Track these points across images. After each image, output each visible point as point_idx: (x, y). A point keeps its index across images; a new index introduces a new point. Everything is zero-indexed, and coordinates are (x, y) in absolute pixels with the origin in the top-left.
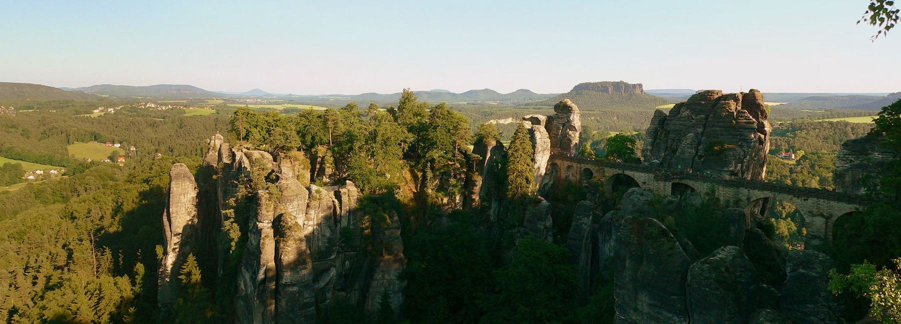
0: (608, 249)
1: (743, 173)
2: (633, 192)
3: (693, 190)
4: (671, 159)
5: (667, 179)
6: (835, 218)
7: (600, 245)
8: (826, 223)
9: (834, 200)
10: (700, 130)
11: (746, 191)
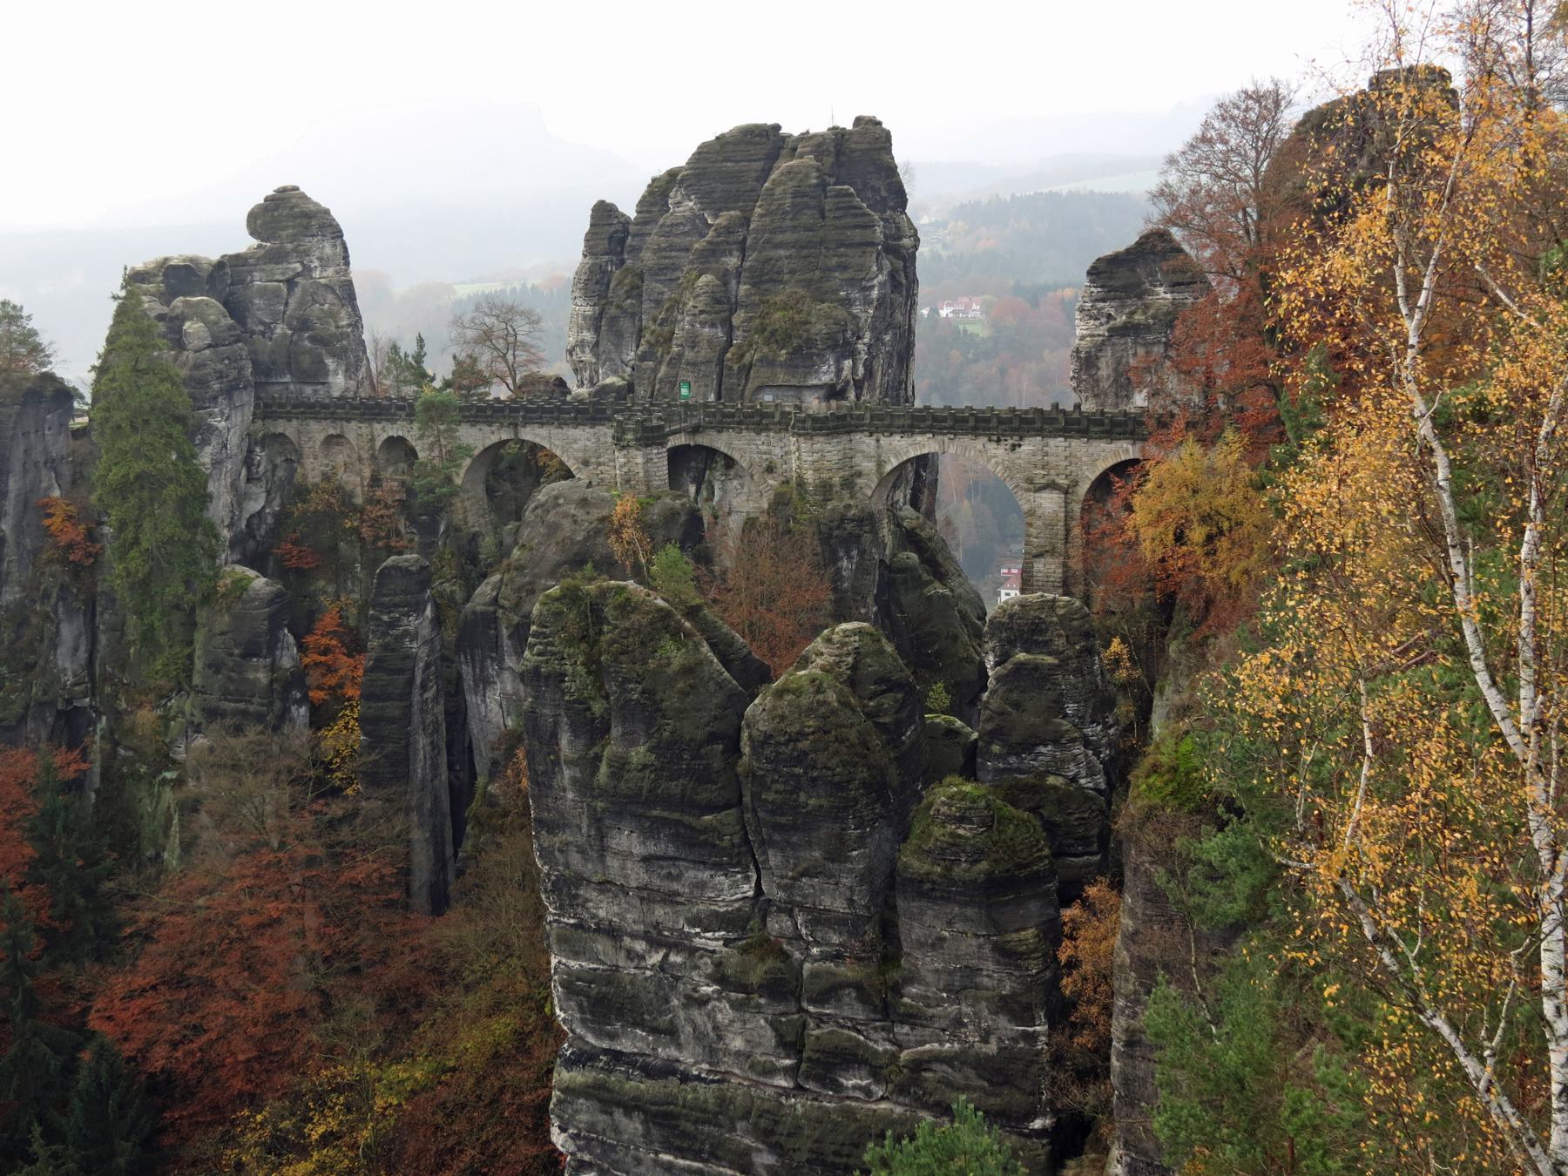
0: (494, 707)
1: (859, 386)
2: (557, 498)
3: (730, 462)
4: (655, 371)
5: (650, 437)
6: (1083, 488)
7: (472, 699)
8: (1066, 503)
9: (1055, 434)
10: (732, 261)
11: (871, 441)
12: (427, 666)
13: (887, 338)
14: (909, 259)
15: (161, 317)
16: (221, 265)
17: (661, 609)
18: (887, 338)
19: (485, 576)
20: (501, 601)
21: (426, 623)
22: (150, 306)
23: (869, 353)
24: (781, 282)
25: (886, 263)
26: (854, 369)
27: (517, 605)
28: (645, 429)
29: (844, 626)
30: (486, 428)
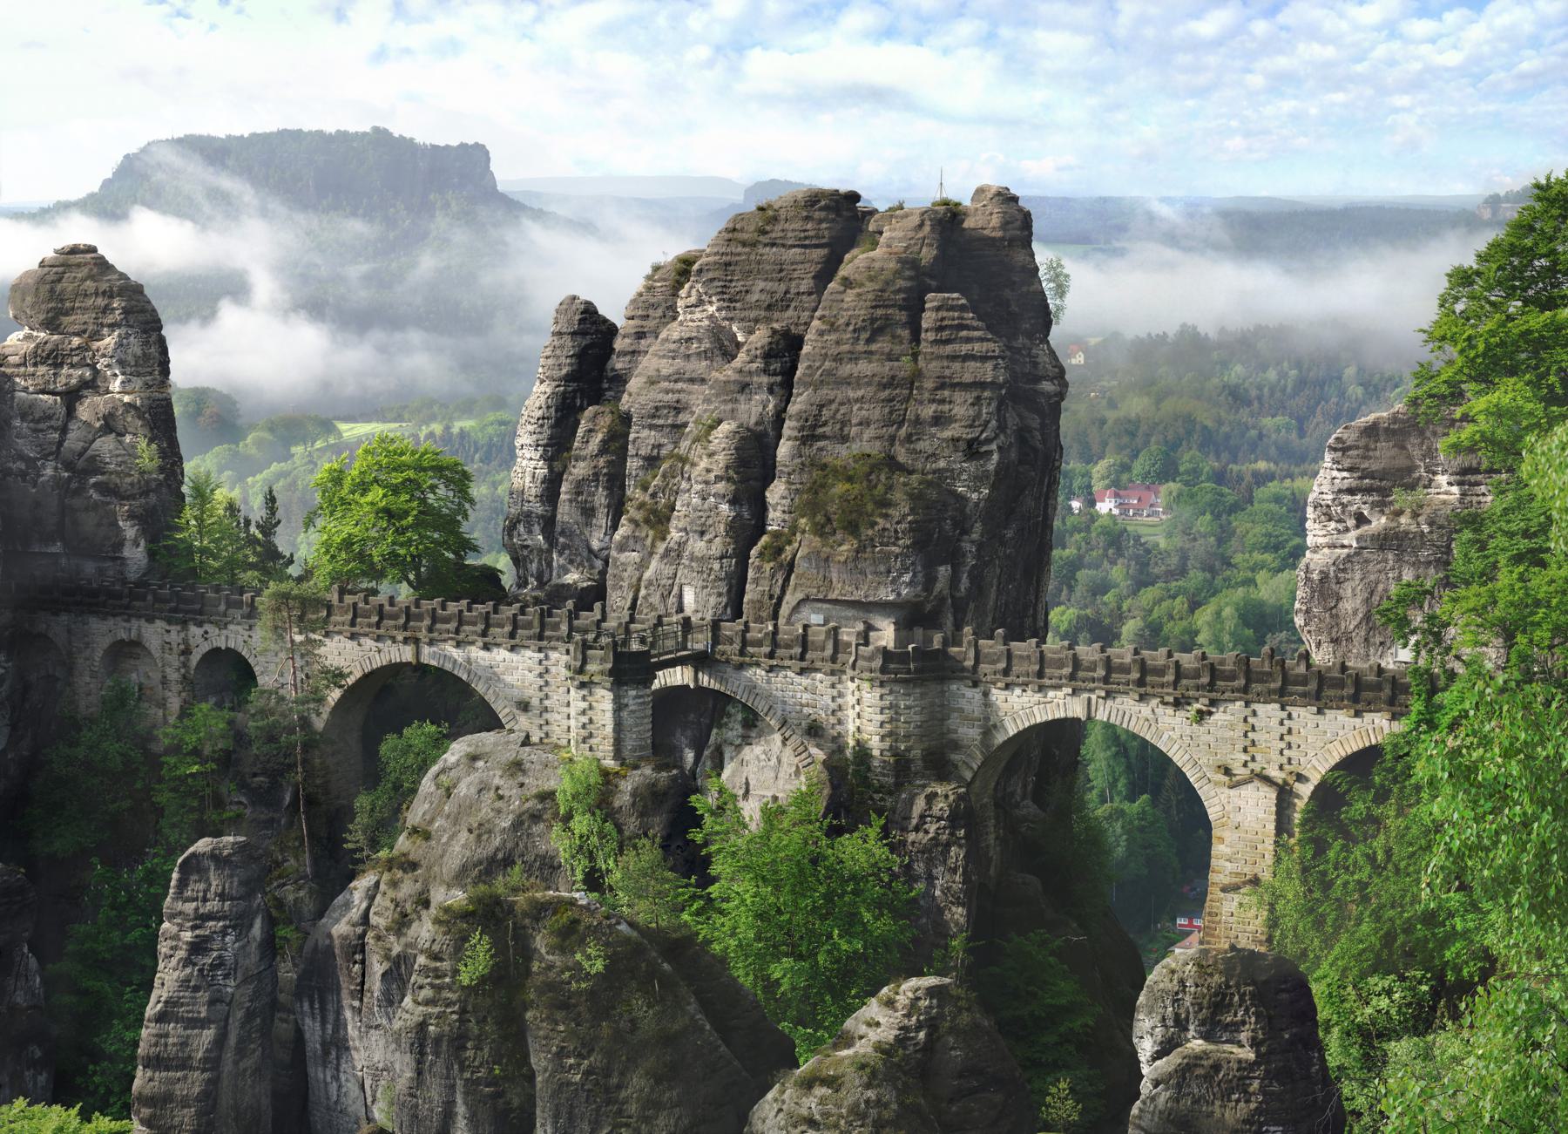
2: (474, 758)
4: (642, 565)
7: (318, 1073)
11: (974, 695)
12: (250, 1015)
13: (1009, 534)
14: (1052, 410)
17: (628, 940)
18: (1009, 534)
19: (352, 876)
20: (374, 920)
21: (254, 945)
23: (978, 556)
24: (844, 439)
25: (1012, 420)
26: (954, 581)
27: (402, 923)
28: (618, 657)
29: (914, 982)
30: (368, 643)
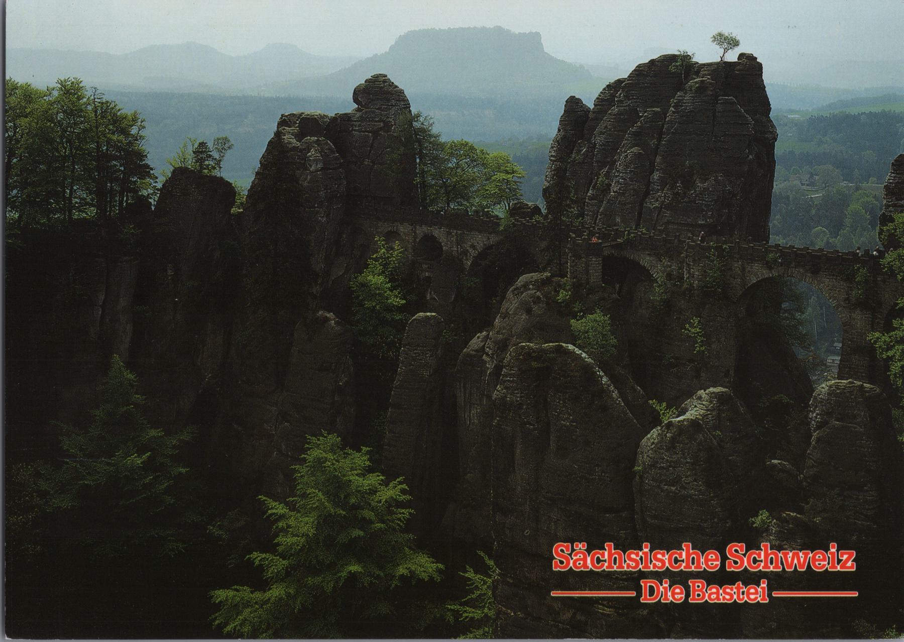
15: (295, 148)
16: (334, 120)
22: (289, 139)
